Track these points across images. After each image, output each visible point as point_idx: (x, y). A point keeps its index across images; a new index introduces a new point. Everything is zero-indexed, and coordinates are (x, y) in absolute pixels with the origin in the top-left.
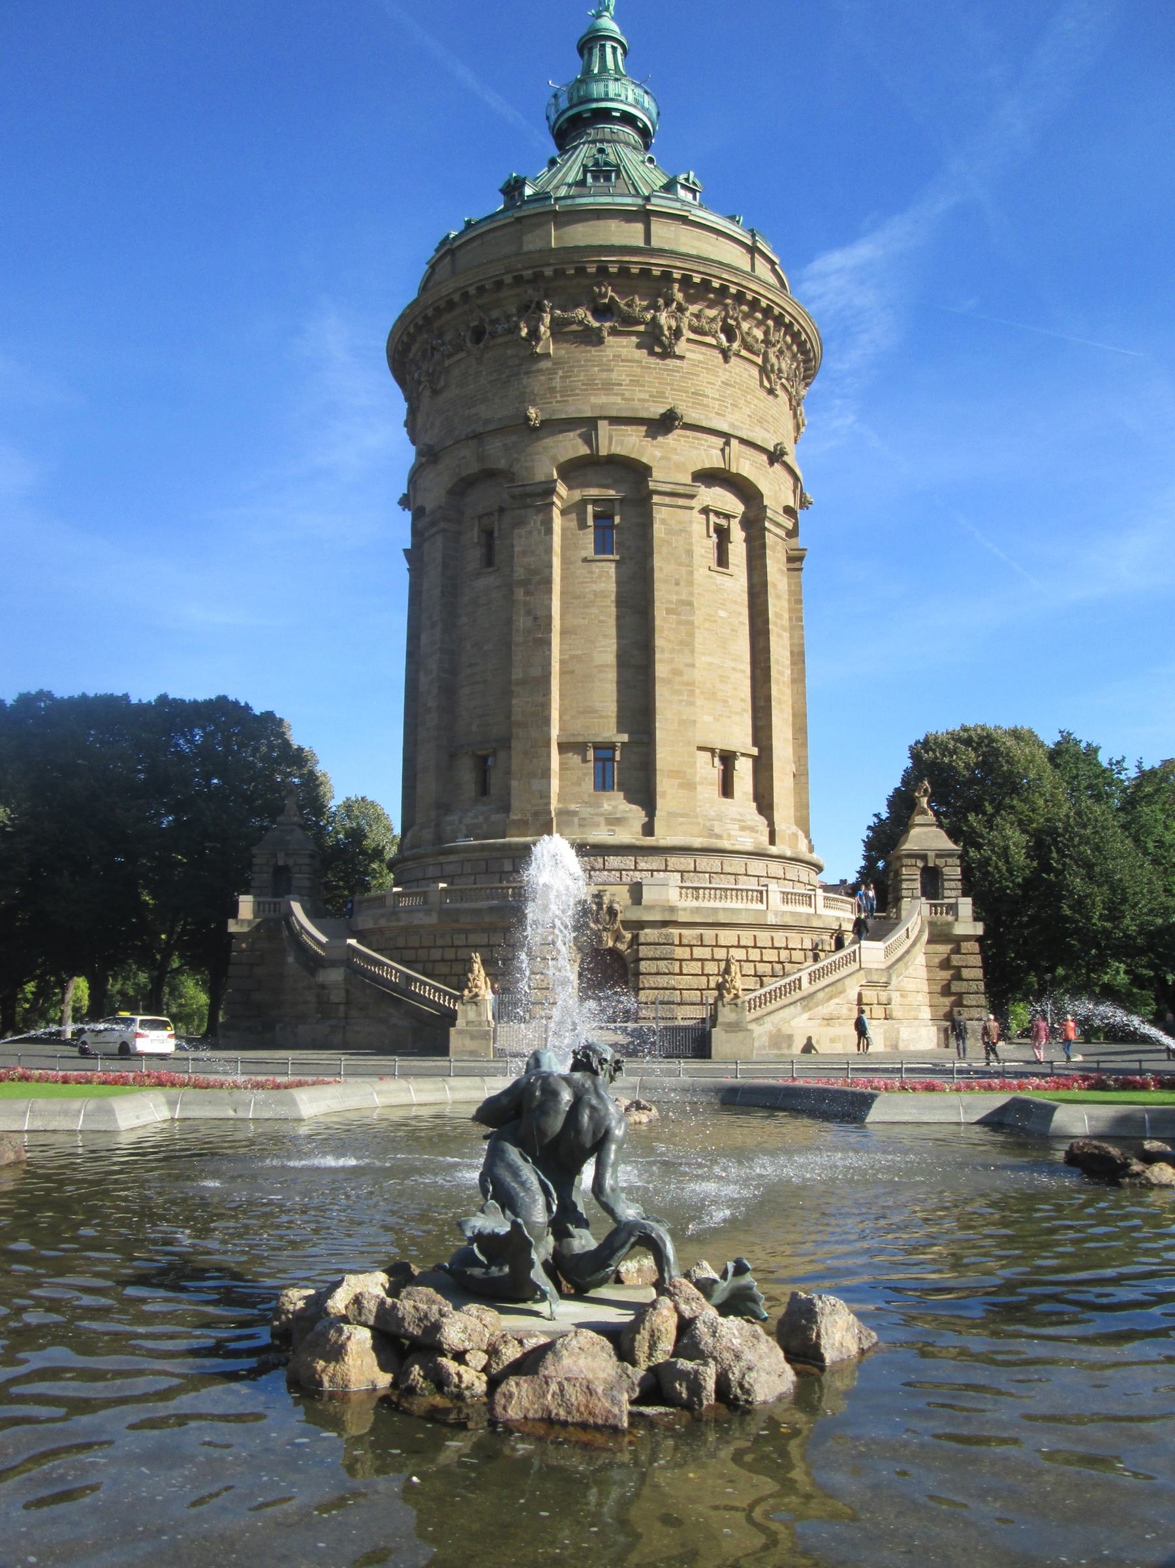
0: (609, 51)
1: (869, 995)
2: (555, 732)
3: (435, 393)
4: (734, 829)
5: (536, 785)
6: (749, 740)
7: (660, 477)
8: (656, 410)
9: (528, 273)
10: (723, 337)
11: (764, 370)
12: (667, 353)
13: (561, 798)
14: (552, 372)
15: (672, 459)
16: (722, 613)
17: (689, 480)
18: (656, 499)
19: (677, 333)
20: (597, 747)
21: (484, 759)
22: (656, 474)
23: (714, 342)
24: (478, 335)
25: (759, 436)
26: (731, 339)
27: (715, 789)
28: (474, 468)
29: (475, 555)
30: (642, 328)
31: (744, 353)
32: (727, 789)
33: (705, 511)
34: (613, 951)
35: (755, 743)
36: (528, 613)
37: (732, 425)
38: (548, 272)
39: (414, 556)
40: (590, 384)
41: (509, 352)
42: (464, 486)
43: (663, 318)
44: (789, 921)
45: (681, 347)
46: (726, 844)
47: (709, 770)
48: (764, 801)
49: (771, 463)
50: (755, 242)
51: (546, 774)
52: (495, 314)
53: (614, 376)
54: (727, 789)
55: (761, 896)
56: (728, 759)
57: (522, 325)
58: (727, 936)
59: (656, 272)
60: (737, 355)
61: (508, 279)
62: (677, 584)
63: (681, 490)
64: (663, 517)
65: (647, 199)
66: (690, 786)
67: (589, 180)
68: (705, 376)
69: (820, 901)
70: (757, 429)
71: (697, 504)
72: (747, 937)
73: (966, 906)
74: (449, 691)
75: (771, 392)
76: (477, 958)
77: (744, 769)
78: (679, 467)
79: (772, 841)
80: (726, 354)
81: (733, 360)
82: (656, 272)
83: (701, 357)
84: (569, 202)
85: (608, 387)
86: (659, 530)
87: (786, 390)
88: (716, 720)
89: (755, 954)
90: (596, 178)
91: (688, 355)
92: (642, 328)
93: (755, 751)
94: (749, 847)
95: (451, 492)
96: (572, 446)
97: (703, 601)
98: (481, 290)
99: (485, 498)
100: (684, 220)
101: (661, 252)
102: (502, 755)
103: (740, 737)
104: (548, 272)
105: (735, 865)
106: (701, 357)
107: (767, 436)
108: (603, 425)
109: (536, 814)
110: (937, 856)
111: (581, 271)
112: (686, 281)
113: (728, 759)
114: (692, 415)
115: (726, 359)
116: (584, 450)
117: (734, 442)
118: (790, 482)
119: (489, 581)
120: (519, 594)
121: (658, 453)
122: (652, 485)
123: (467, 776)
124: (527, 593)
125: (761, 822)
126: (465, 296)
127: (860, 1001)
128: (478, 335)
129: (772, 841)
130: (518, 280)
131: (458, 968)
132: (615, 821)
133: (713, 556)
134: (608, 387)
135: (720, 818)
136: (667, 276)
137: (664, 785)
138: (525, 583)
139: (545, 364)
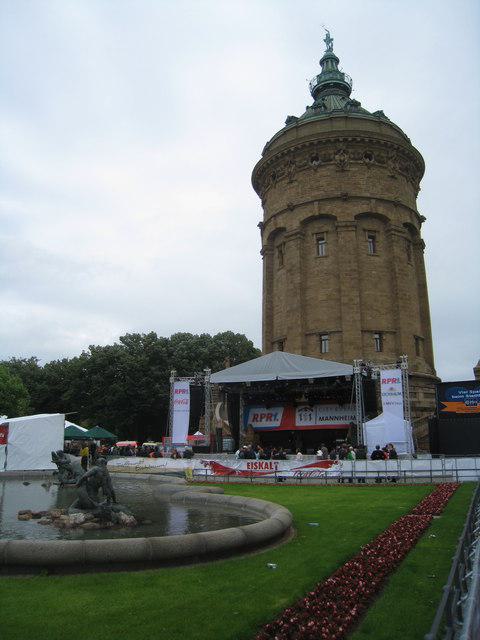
12: (343, 171)
24: (274, 177)
25: (386, 197)
29: (277, 262)
59: (332, 140)
62: (350, 262)
63: (349, 224)
75: (392, 177)
77: (387, 338)
82: (332, 140)
87: (404, 176)
112: (345, 140)
114: (353, 193)
115: (369, 168)
116: (310, 215)
119: (283, 271)
121: (339, 211)
128: (274, 177)
134: (318, 188)
139: (296, 184)
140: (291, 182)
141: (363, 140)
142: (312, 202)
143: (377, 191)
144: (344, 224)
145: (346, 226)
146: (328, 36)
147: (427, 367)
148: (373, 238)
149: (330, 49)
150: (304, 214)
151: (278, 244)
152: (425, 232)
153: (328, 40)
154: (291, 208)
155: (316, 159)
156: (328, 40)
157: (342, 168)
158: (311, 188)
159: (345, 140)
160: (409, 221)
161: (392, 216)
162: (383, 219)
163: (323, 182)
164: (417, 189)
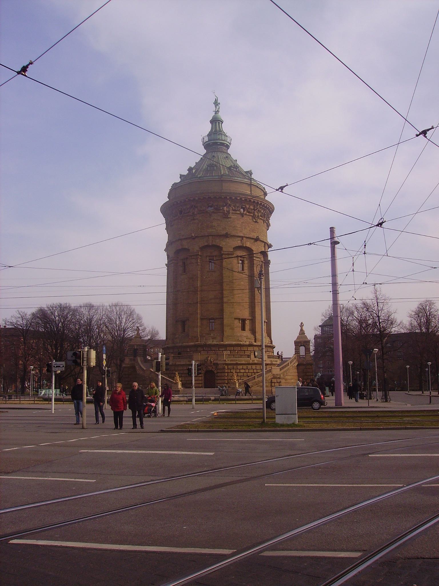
0: (217, 124)
1: (274, 380)
4: (245, 340)
10: (242, 210)
11: (254, 217)
15: (228, 245)
16: (242, 283)
17: (232, 250)
19: (228, 212)
22: (224, 249)
28: (180, 248)
31: (247, 214)
34: (211, 370)
38: (197, 199)
44: (256, 362)
45: (230, 215)
47: (238, 324)
48: (253, 331)
50: (251, 182)
54: (243, 329)
55: (249, 356)
56: (243, 321)
58: (241, 367)
60: (246, 214)
65: (222, 176)
66: (232, 329)
72: (245, 367)
75: (256, 222)
76: (177, 373)
80: (242, 215)
81: (245, 216)
86: (224, 264)
89: (247, 371)
91: (233, 217)
94: (248, 343)
104: (197, 199)
105: (245, 348)
113: (243, 321)
114: (233, 233)
121: (224, 244)
125: (252, 336)
127: (271, 382)
131: (173, 375)
132: (214, 338)
135: (241, 336)
137: (226, 329)
140: (194, 219)
141: (241, 199)
142: (208, 236)
143: (246, 232)
144: (227, 253)
145: (228, 254)
146: (216, 101)
147: (268, 339)
149: (217, 112)
150: (203, 243)
152: (271, 256)
153: (216, 103)
154: (194, 238)
155: (211, 207)
156: (216, 103)
163: (215, 224)
164: (268, 225)
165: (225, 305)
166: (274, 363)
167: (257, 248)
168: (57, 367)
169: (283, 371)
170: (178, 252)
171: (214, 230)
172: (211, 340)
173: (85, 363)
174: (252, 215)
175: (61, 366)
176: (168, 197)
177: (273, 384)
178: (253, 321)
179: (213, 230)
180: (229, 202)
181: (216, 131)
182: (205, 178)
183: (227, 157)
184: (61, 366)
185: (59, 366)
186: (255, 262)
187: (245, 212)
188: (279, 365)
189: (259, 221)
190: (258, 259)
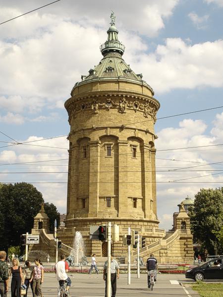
2: (98, 195)
3: (74, 118)
5: (94, 206)
6: (141, 195)
7: (121, 139)
8: (120, 125)
9: (93, 96)
12: (123, 113)
13: (99, 209)
14: (98, 117)
15: (123, 136)
18: (120, 144)
20: (107, 197)
21: (84, 199)
22: (120, 139)
23: (132, 108)
25: (142, 129)
26: (137, 107)
27: (132, 206)
29: (82, 155)
30: (118, 107)
31: (139, 110)
32: (135, 206)
33: (131, 145)
35: (142, 196)
36: (93, 169)
37: (136, 127)
38: (97, 96)
39: (70, 151)
40: (106, 119)
41: (90, 112)
42: (79, 141)
43: (121, 105)
46: (134, 219)
47: (131, 202)
49: (146, 133)
51: (96, 204)
52: (87, 103)
53: (111, 118)
54: (135, 206)
56: (135, 199)
57: (92, 106)
60: (138, 110)
61: (89, 97)
63: (125, 142)
64: (121, 148)
65: (119, 77)
66: (126, 206)
67: (107, 71)
68: (131, 116)
69: (154, 231)
70: (142, 126)
71: (129, 145)
73: (189, 231)
74: (77, 184)
75: (146, 117)
77: (139, 202)
78: (125, 137)
79: (145, 218)
80: (135, 111)
83: (129, 112)
84: (102, 79)
85: (110, 120)
88: (133, 191)
90: (109, 71)
92: (118, 107)
93: (142, 197)
94: (139, 219)
95: (78, 141)
96: (102, 133)
97: (130, 163)
98: (84, 98)
99: (83, 144)
100: (126, 82)
101: (121, 92)
102: (87, 199)
103: (138, 194)
104: (97, 96)
105: (136, 223)
106: (129, 112)
107: (144, 127)
108: (109, 129)
109: (94, 213)
110: (185, 219)
111: (104, 96)
112: (126, 96)
113: (135, 199)
115: (135, 112)
116: (105, 134)
117: (137, 130)
118: (151, 136)
120: (91, 164)
122: (119, 142)
123: (80, 203)
124: (93, 165)
126: (81, 99)
128: (83, 107)
129: (145, 218)
130: (91, 97)
133: (132, 155)
134: (110, 120)
135: (133, 212)
136: (122, 96)
138: (92, 162)
139: (97, 115)
144: (122, 142)
148: (135, 150)
151: (84, 145)
157: (121, 111)
158: (106, 119)
159: (126, 96)
160: (151, 140)
161: (144, 139)
162: (140, 140)
165: (120, 186)
166: (161, 236)
167: (146, 139)
168: (31, 240)
169: (168, 243)
170: (75, 139)
171: (112, 123)
172: (108, 216)
173: (110, 238)
174: (143, 111)
175: (36, 239)
176: (72, 94)
177: (161, 255)
178: (143, 200)
179: (110, 123)
180: (125, 100)
181: (112, 40)
182: (104, 79)
183: (122, 62)
184: (36, 239)
185: (34, 240)
186: (145, 150)
187: (137, 108)
188: (164, 238)
189: (148, 116)
190: (147, 148)
